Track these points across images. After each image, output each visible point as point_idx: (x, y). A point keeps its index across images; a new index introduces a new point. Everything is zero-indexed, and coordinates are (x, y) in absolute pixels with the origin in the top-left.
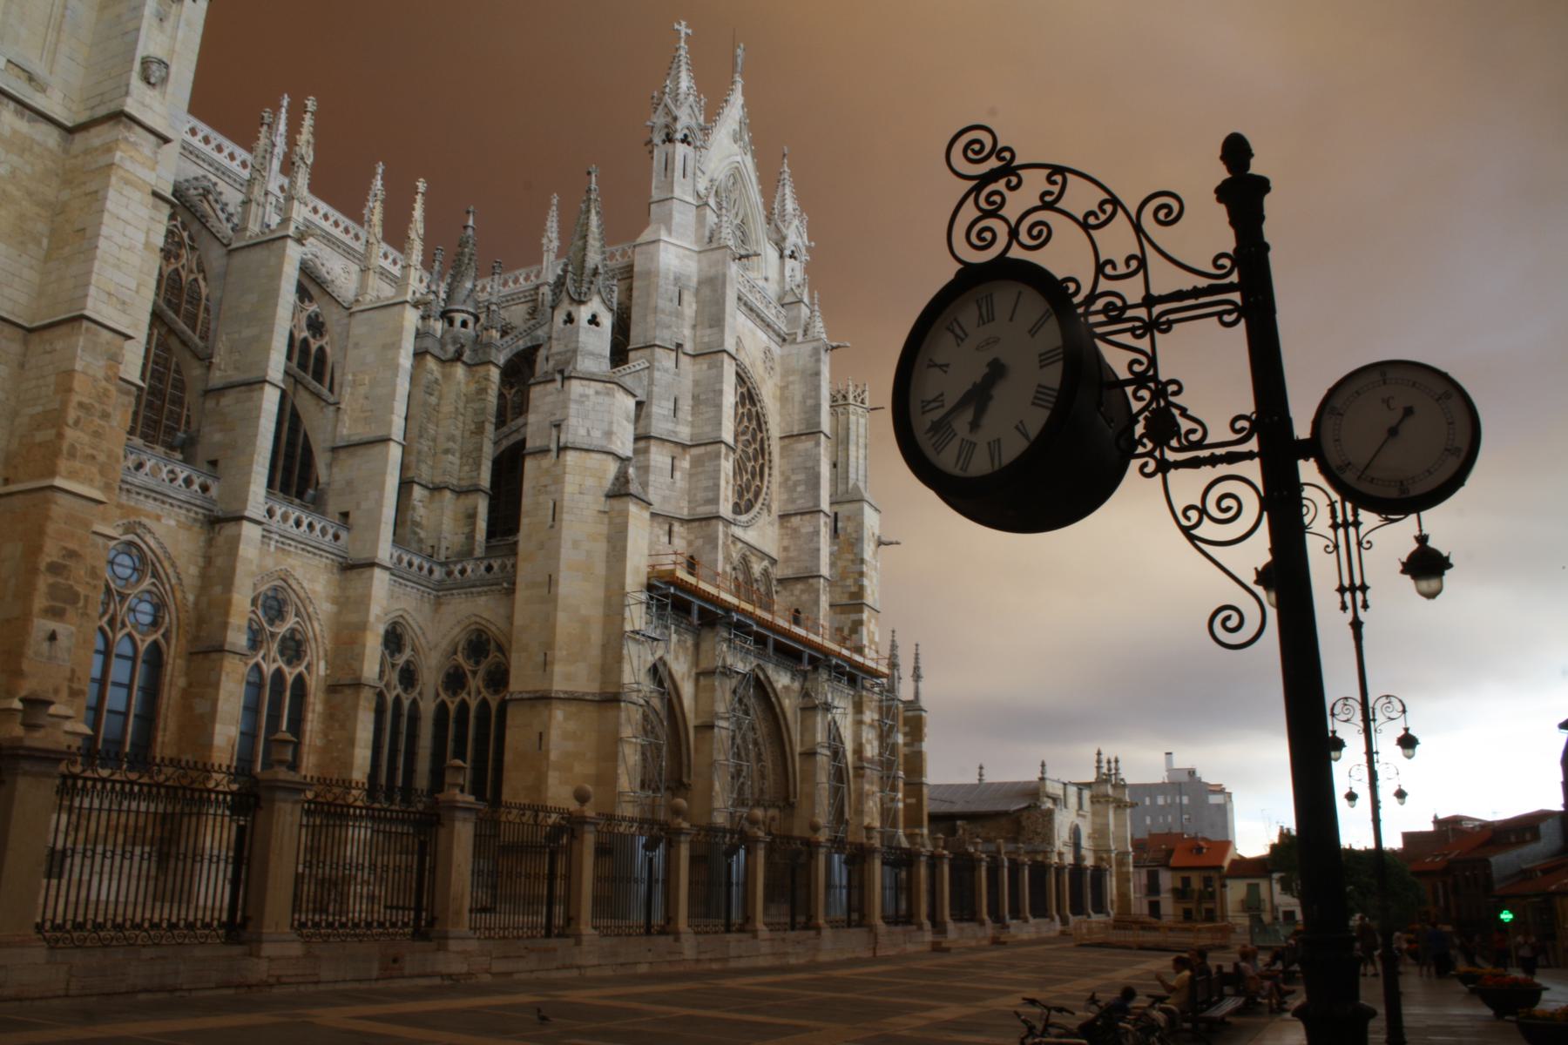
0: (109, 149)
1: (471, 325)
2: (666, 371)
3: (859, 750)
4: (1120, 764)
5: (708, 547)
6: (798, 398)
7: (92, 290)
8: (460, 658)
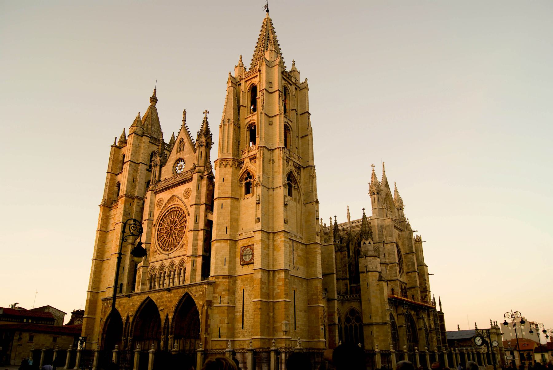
0: (315, 249)
1: (340, 242)
2: (382, 248)
3: (430, 326)
4: (497, 323)
5: (396, 286)
6: (407, 244)
7: (318, 273)
8: (349, 315)
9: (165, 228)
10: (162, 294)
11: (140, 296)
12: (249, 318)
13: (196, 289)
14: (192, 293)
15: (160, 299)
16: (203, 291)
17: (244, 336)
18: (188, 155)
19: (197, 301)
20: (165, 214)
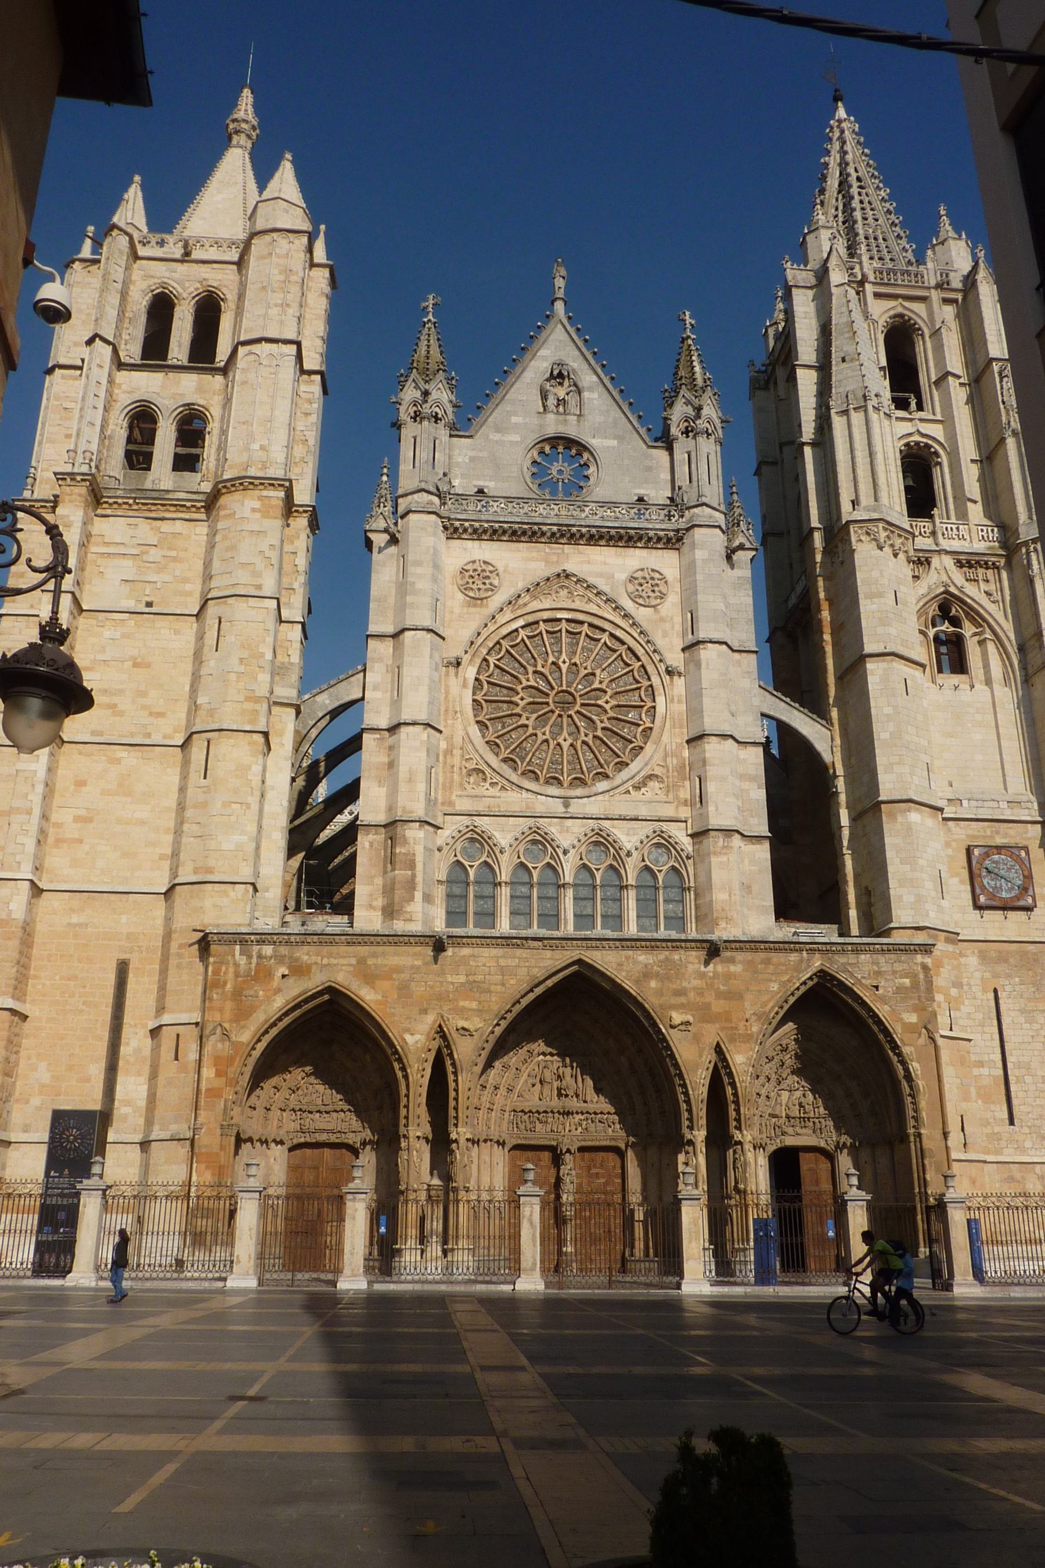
9: (523, 689)
10: (667, 959)
11: (519, 952)
12: (1032, 1088)
13: (877, 964)
14: (851, 974)
15: (668, 978)
16: (914, 976)
17: (1023, 1150)
18: (614, 443)
19: (887, 1008)
20: (516, 630)
